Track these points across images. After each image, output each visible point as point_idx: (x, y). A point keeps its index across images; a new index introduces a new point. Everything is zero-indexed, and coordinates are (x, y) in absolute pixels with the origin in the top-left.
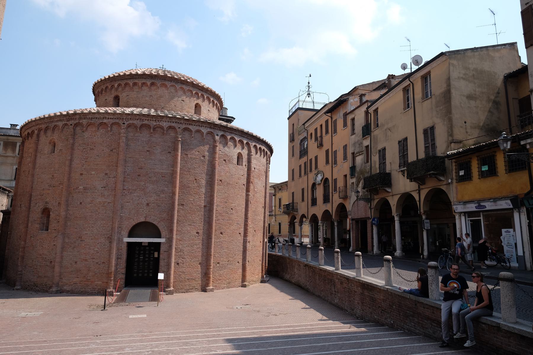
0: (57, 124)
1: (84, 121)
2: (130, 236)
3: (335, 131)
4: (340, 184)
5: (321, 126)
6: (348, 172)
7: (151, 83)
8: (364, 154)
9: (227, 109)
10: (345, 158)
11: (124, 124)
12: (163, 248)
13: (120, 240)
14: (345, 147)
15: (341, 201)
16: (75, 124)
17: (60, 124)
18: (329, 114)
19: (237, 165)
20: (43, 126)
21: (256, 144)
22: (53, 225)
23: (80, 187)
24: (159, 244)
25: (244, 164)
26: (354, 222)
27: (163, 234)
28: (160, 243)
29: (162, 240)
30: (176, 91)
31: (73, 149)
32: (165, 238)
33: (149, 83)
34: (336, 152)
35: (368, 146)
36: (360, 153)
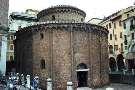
0: (44, 27)
1: (56, 26)
2: (77, 69)
3: (115, 27)
4: (120, 47)
5: (107, 25)
6: (123, 42)
8: (131, 37)
10: (121, 37)
12: (88, 73)
13: (74, 71)
14: (121, 34)
15: (120, 53)
17: (46, 27)
18: (112, 21)
20: (37, 28)
23: (57, 52)
24: (87, 71)
26: (127, 61)
27: (88, 68)
30: (76, 14)
33: (67, 11)
34: (116, 35)
35: (133, 33)
36: (129, 36)
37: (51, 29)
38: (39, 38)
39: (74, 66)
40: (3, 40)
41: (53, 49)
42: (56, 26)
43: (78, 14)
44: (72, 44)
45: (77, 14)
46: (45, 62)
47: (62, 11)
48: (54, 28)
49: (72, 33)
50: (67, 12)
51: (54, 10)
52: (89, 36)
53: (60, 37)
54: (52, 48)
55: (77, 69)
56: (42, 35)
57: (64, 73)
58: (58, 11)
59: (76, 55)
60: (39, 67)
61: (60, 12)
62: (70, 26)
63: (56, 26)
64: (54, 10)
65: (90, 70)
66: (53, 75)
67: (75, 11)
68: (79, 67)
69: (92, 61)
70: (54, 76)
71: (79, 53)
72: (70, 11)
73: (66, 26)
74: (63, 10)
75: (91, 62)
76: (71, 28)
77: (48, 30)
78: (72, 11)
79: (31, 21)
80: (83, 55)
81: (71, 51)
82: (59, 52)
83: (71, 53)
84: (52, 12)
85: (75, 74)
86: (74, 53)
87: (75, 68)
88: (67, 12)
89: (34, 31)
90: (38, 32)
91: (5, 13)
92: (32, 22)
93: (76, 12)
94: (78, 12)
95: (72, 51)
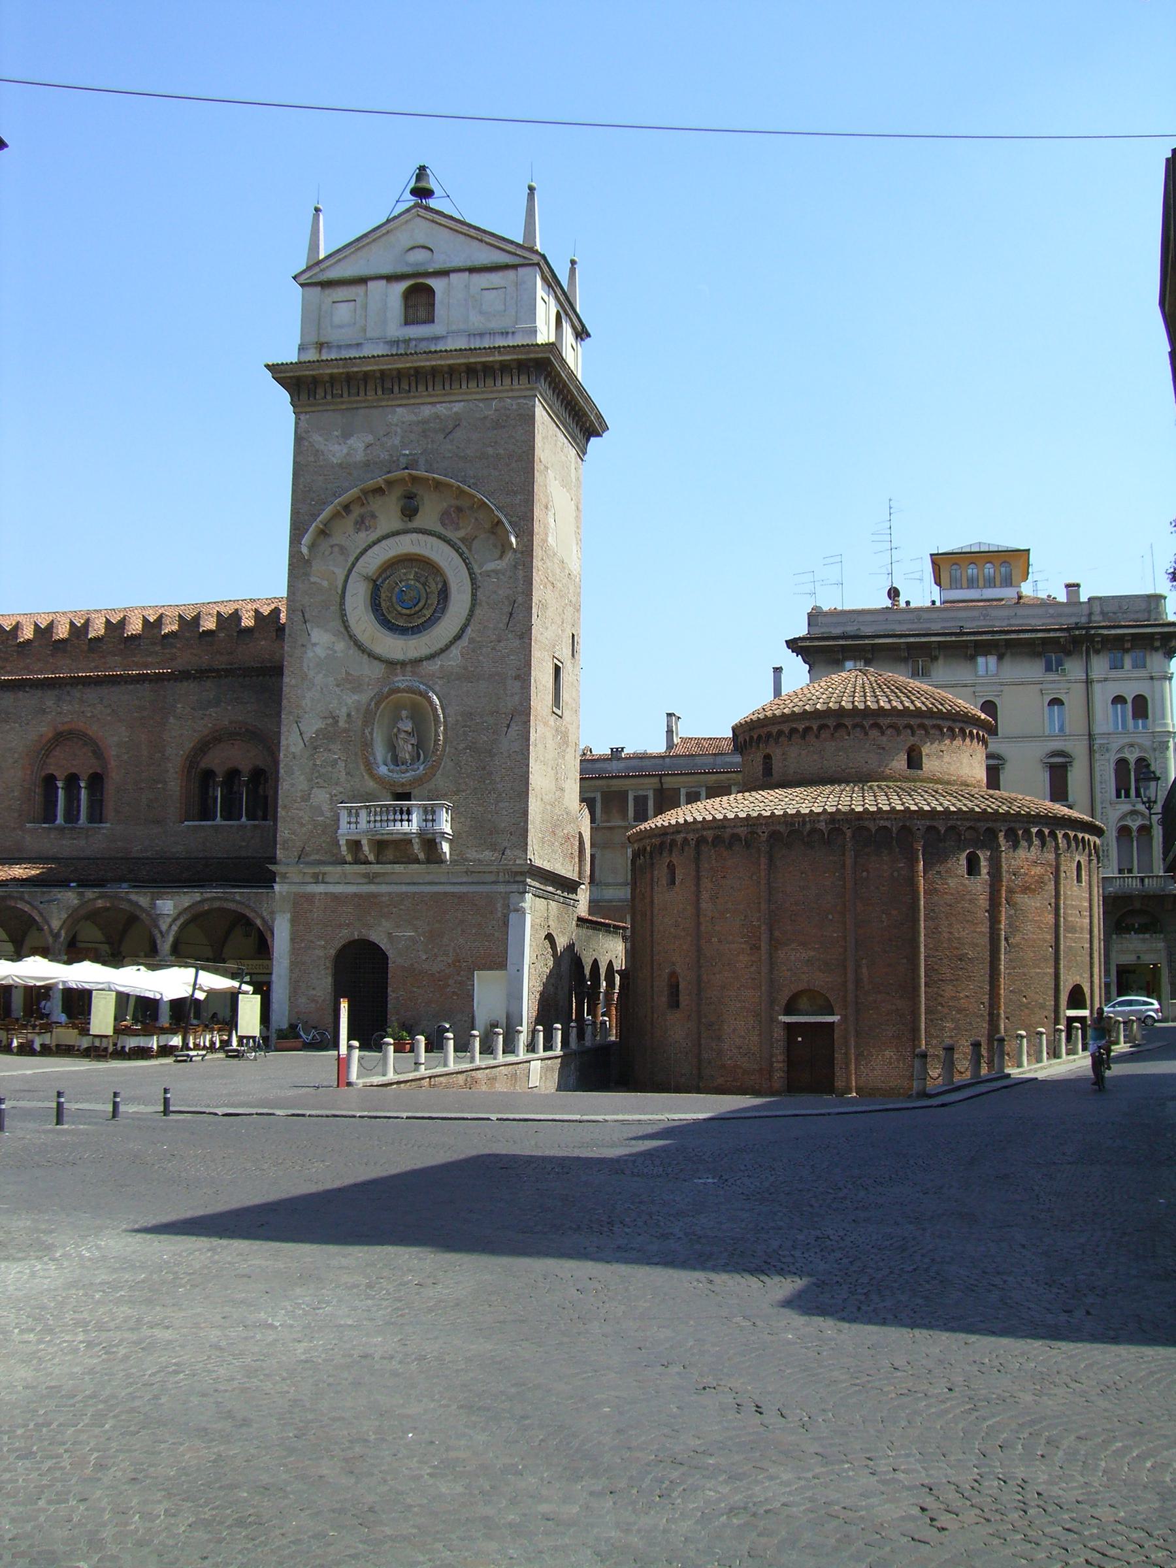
0: (674, 837)
7: (819, 726)
9: (1165, 598)
11: (763, 832)
13: (773, 1020)
16: (697, 839)
17: (679, 838)
19: (969, 873)
21: (1013, 825)
22: (684, 999)
25: (984, 871)
28: (834, 1022)
29: (835, 1019)
30: (866, 734)
31: (698, 878)
32: (840, 1015)
37: (693, 843)
38: (665, 883)
39: (772, 1002)
40: (512, 907)
41: (703, 928)
42: (709, 834)
43: (883, 733)
44: (763, 906)
45: (874, 733)
46: (680, 980)
47: (793, 731)
48: (701, 841)
49: (763, 860)
50: (817, 737)
51: (765, 730)
52: (844, 866)
53: (724, 877)
54: (699, 924)
55: (788, 1011)
56: (672, 868)
57: (734, 1030)
58: (780, 733)
59: (781, 954)
60: (663, 1000)
61: (790, 738)
62: (759, 831)
63: (709, 834)
64: (765, 730)
65: (844, 1018)
66: (699, 1033)
67: (858, 720)
68: (803, 1003)
69: (858, 982)
70: (703, 1042)
71: (793, 946)
72: (828, 727)
73: (742, 831)
74: (801, 727)
75: (851, 986)
76: (764, 837)
77: (686, 848)
78: (839, 726)
79: (934, 659)
80: (812, 954)
81: (760, 939)
82: (720, 941)
83: (759, 948)
84: (760, 737)
85: (779, 1033)
86: (775, 944)
87: (777, 1008)
88: (817, 737)
89: (651, 853)
90: (661, 854)
91: (516, 808)
92: (941, 661)
93: (863, 727)
94: (876, 725)
95: (765, 937)
